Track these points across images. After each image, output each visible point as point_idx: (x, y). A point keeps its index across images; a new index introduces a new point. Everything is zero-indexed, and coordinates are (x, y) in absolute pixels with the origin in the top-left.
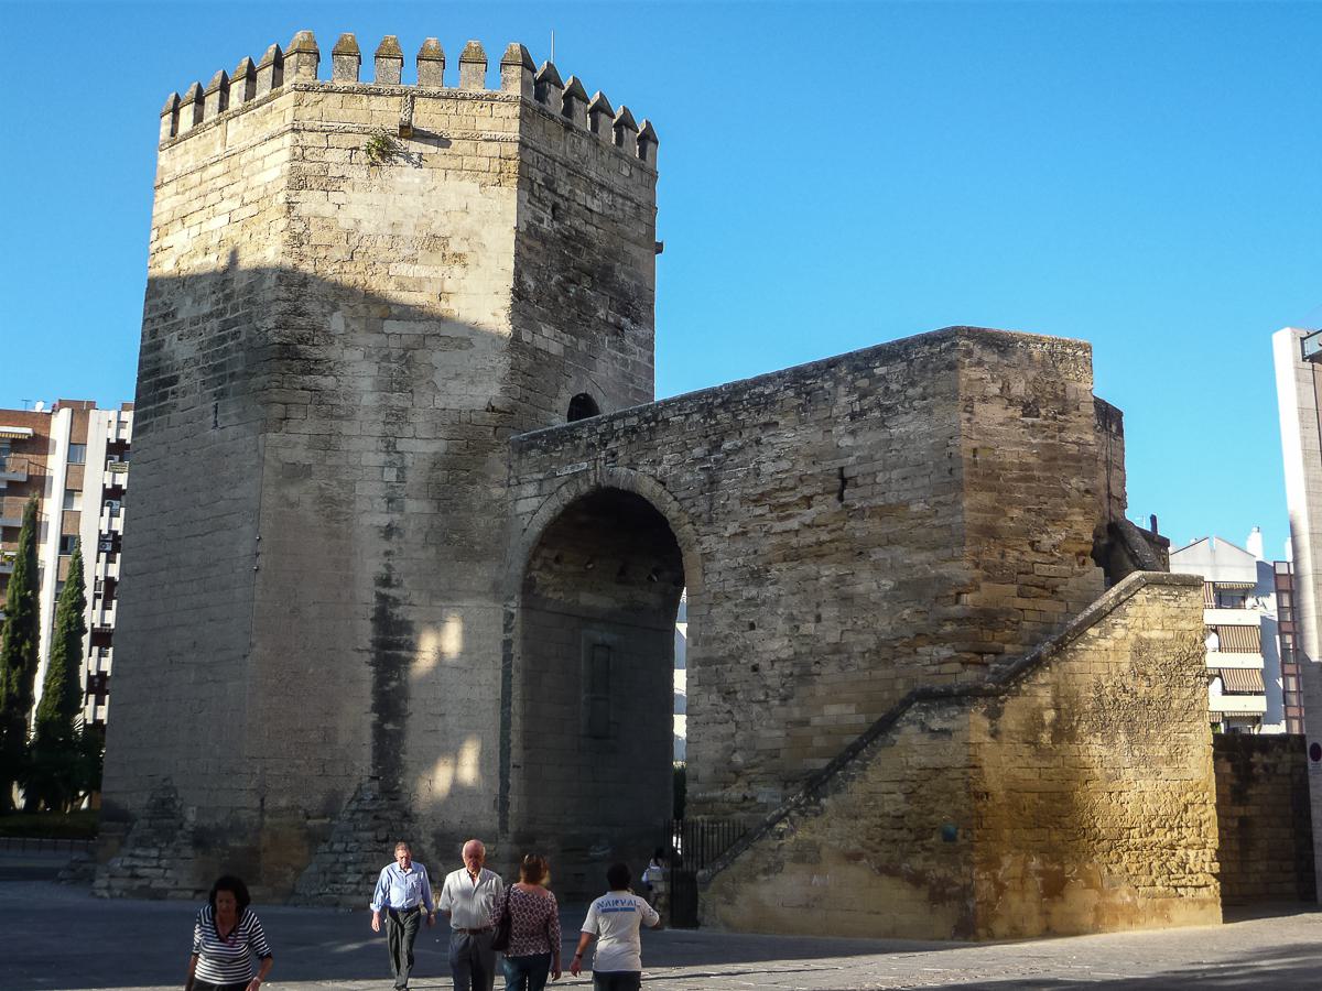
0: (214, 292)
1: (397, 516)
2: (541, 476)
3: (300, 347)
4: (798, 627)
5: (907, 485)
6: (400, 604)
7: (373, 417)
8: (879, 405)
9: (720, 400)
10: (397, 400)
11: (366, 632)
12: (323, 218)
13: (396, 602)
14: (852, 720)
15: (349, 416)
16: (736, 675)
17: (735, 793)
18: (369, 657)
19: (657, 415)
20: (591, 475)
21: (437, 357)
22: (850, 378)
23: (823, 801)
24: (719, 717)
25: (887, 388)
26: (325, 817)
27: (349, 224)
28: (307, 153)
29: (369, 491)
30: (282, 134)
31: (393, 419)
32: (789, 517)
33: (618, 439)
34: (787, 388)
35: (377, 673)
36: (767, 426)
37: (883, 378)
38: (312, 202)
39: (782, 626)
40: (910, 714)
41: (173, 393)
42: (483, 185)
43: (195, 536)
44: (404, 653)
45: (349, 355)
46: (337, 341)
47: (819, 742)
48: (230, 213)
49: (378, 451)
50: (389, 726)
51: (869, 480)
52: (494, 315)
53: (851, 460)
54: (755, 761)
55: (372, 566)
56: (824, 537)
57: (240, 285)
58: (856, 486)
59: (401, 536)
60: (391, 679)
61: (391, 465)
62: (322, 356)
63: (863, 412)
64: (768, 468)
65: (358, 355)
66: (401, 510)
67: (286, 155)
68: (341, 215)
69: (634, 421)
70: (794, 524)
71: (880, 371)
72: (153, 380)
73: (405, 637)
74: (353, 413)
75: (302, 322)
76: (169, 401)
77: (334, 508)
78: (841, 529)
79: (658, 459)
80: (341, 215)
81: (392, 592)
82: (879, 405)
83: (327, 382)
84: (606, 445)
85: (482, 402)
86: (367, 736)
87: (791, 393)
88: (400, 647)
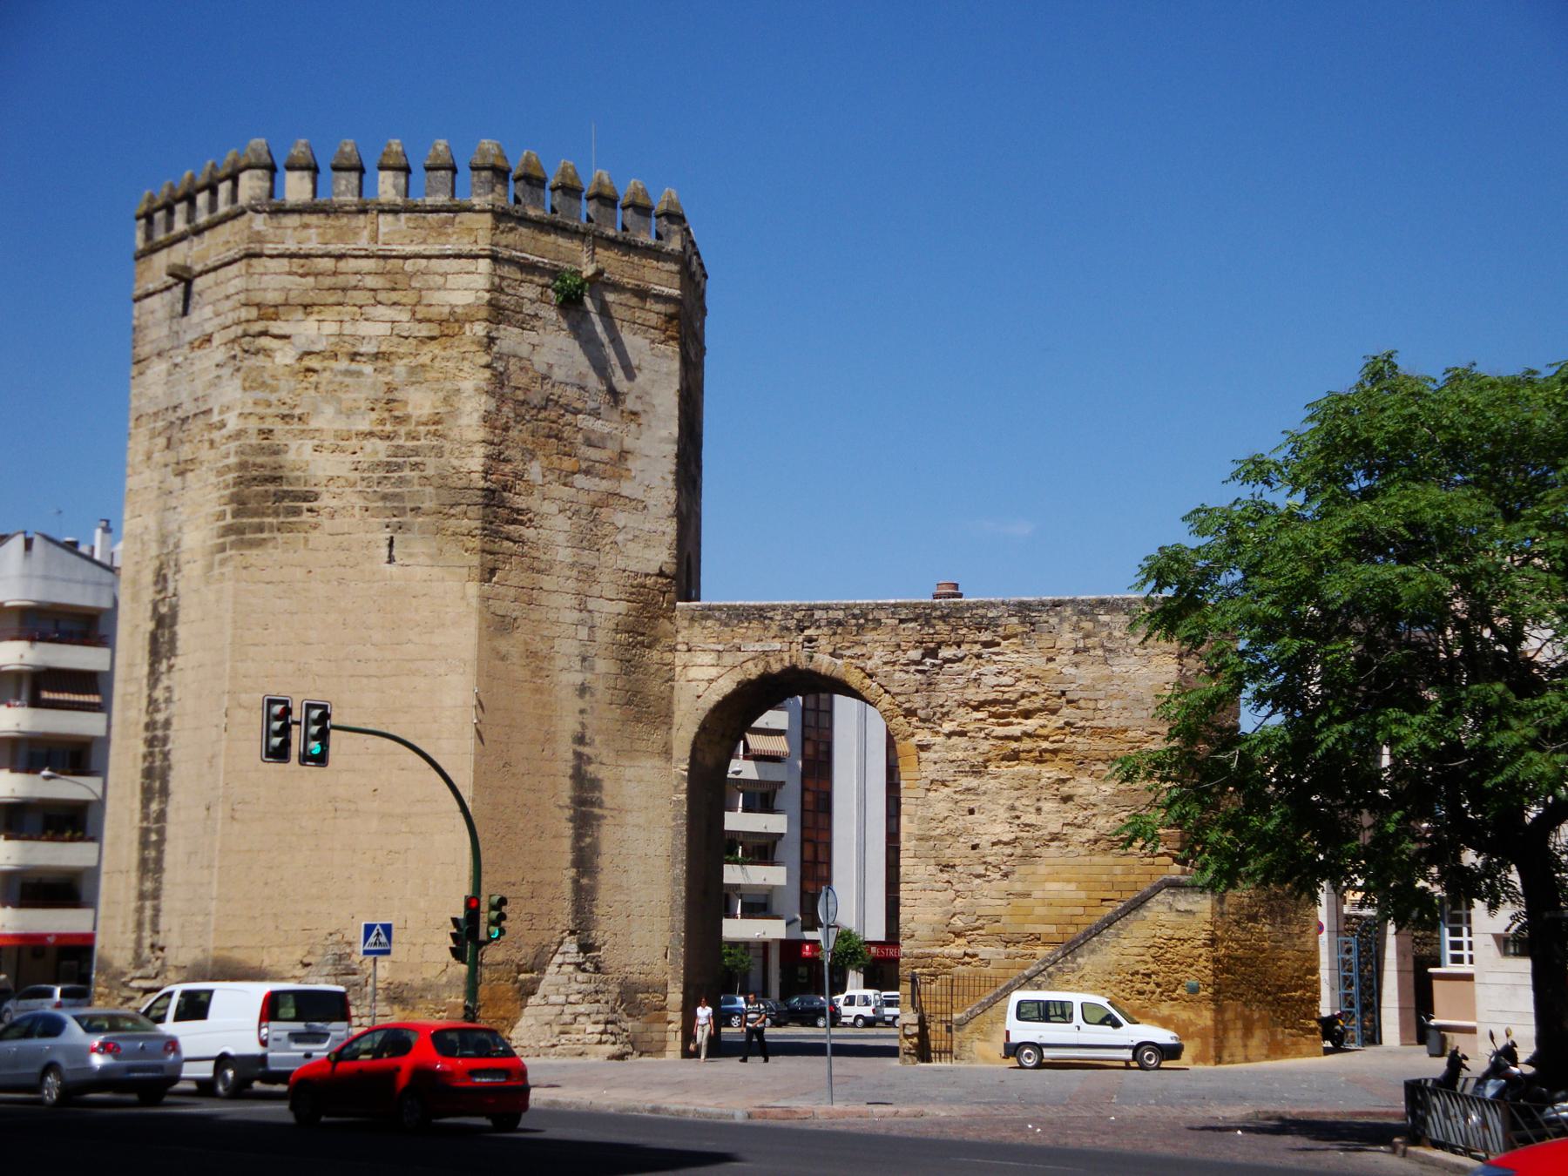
0: (373, 409)
1: (589, 676)
2: (720, 647)
3: (505, 494)
4: (1018, 817)
5: (1126, 714)
7: (568, 573)
8: (1102, 646)
9: (938, 613)
10: (588, 557)
11: (566, 790)
12: (521, 359)
13: (589, 761)
14: (1073, 895)
16: (957, 851)
17: (956, 949)
18: (569, 813)
19: (867, 614)
20: (786, 656)
21: (621, 519)
22: (1075, 618)
23: (1079, 960)
24: (938, 886)
25: (1110, 634)
26: (532, 971)
27: (543, 369)
28: (505, 284)
29: (567, 648)
30: (477, 257)
31: (583, 577)
32: (1011, 724)
33: (819, 627)
34: (1010, 616)
35: (575, 828)
36: (986, 645)
37: (1107, 625)
38: (510, 337)
39: (1003, 814)
40: (1160, 897)
41: (310, 510)
42: (653, 342)
43: (368, 676)
44: (596, 811)
45: (549, 508)
47: (1041, 911)
49: (572, 608)
50: (584, 881)
51: (1091, 705)
52: (663, 478)
53: (1074, 686)
54: (977, 924)
55: (568, 725)
56: (1045, 745)
58: (1079, 708)
59: (592, 695)
60: (585, 835)
61: (582, 623)
63: (1086, 649)
64: (990, 680)
65: (554, 508)
66: (592, 669)
67: (482, 282)
68: (535, 359)
69: (840, 615)
70: (1016, 730)
71: (1104, 618)
72: (271, 488)
73: (597, 794)
74: (551, 568)
75: (508, 468)
77: (537, 660)
78: (1062, 741)
79: (868, 655)
81: (586, 750)
82: (1102, 646)
83: (529, 533)
84: (802, 631)
85: (654, 569)
86: (567, 888)
87: (1015, 620)
88: (593, 804)
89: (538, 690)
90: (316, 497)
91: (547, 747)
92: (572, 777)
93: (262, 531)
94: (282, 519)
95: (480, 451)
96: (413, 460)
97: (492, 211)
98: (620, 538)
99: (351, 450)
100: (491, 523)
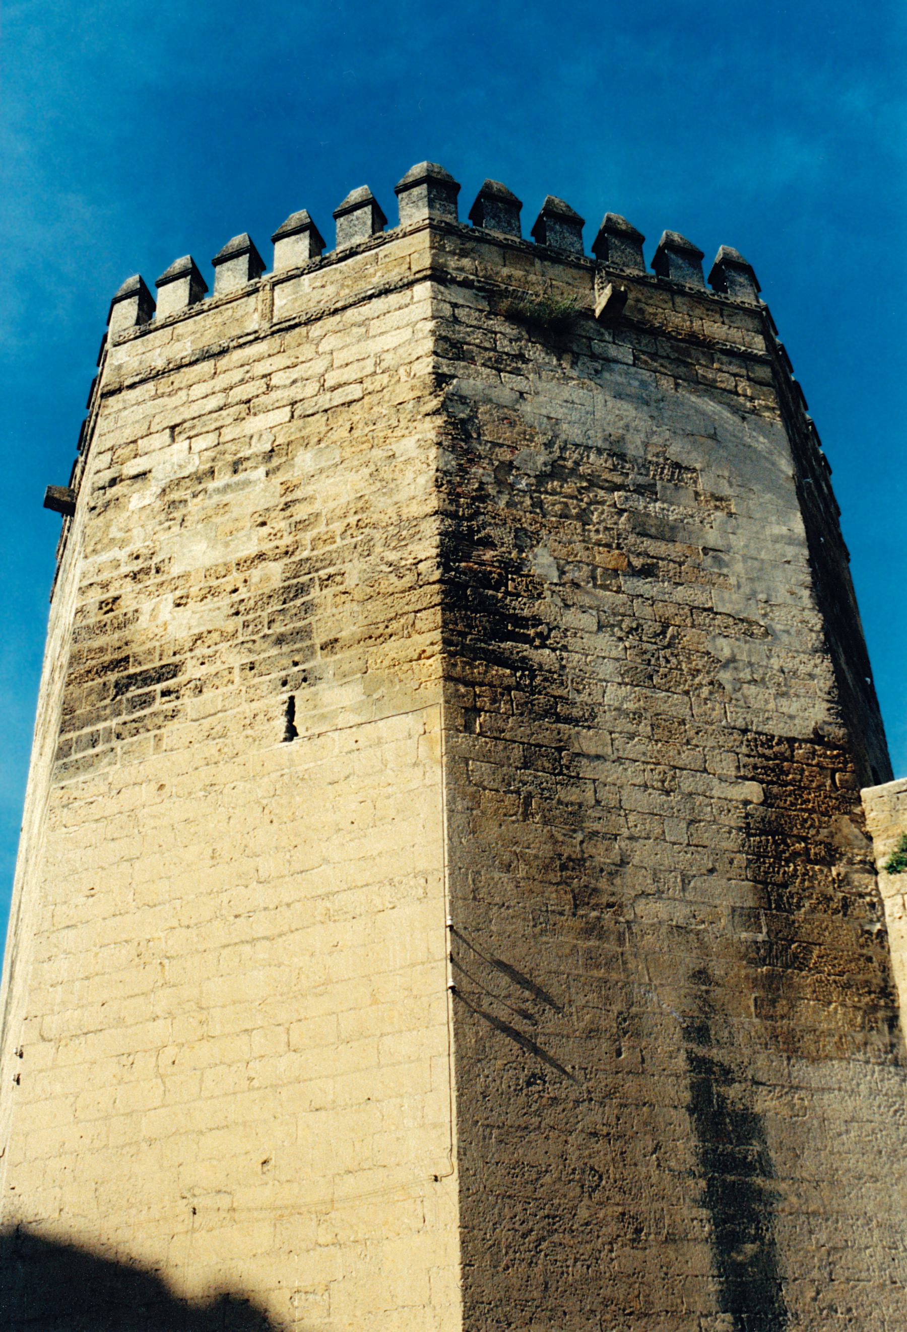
6: (733, 1081)
12: (499, 406)
13: (727, 1075)
15: (588, 720)
30: (410, 285)
35: (718, 1222)
41: (165, 693)
43: (253, 941)
45: (571, 618)
46: (547, 593)
48: (293, 404)
57: (331, 505)
62: (526, 613)
65: (588, 621)
72: (112, 677)
73: (756, 1147)
76: (157, 706)
80: (526, 408)
81: (716, 1054)
83: (545, 656)
88: (748, 1168)
89: (593, 930)
90: (174, 670)
91: (625, 1043)
92: (691, 1110)
93: (94, 743)
94: (125, 717)
95: (432, 528)
96: (323, 573)
97: (430, 226)
98: (725, 676)
99: (230, 588)
100: (463, 635)
